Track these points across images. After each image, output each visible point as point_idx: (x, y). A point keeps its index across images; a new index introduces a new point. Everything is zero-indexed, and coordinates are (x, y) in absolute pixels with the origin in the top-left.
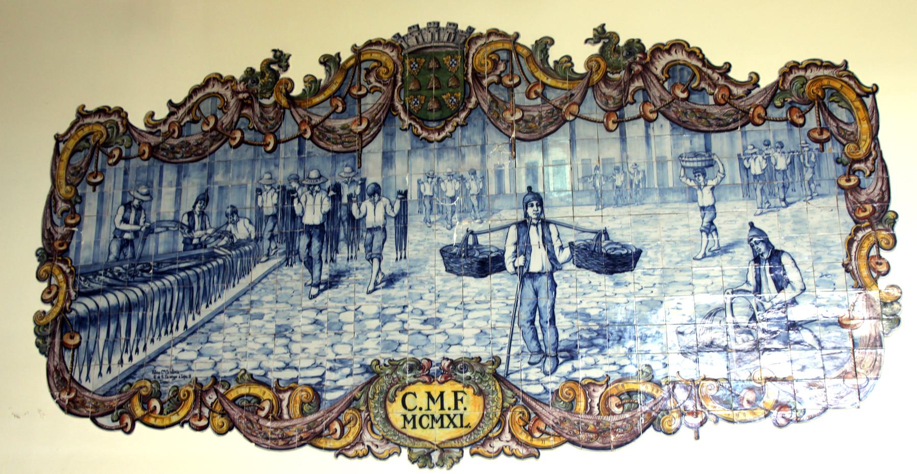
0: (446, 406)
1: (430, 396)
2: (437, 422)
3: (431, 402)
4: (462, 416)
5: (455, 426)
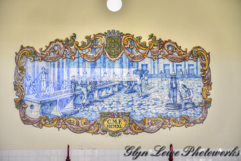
0: (117, 123)
1: (113, 120)
3: (114, 122)
4: (121, 125)
5: (119, 127)
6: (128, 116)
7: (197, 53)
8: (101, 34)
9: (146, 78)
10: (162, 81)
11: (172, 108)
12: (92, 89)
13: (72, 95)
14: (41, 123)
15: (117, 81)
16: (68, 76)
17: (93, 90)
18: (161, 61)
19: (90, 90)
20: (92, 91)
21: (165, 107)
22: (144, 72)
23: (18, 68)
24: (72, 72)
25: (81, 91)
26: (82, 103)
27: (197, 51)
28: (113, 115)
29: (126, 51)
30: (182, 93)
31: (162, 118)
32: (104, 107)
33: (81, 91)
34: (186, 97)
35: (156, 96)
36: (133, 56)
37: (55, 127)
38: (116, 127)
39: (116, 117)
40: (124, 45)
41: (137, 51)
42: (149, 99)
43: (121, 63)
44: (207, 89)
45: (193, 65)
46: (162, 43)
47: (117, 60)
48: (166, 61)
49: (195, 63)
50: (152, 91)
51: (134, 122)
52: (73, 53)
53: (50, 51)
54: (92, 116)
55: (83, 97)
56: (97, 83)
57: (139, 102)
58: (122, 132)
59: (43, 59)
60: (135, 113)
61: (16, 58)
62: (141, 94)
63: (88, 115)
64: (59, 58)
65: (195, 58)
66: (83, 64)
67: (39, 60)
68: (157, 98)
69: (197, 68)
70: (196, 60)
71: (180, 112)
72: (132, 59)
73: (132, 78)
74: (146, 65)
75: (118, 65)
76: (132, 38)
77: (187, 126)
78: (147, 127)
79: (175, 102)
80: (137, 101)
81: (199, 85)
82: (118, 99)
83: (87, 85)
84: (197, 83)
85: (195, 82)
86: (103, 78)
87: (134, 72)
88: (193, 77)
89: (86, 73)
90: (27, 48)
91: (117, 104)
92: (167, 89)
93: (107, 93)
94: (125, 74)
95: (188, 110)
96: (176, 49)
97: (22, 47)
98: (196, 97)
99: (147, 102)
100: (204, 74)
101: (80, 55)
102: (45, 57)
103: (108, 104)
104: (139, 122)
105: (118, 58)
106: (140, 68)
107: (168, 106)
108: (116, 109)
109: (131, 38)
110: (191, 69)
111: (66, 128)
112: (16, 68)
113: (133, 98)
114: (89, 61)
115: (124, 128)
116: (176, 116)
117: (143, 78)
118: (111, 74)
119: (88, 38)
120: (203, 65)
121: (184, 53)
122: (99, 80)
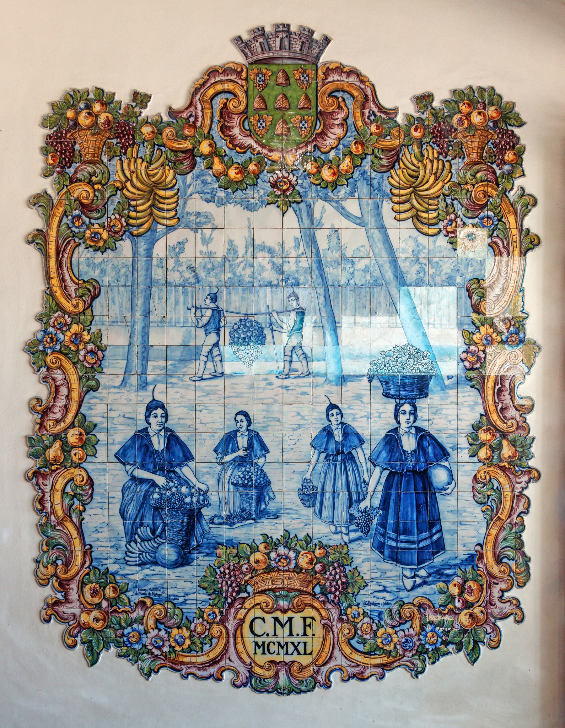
0: (294, 633)
2: (282, 648)
4: (305, 643)
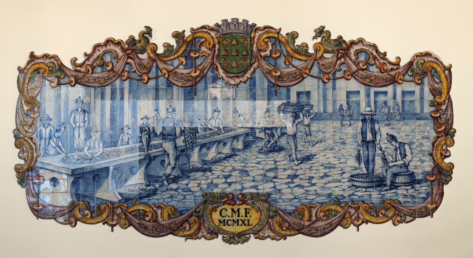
0: (240, 216)
1: (233, 210)
3: (233, 213)
4: (249, 220)
6: (266, 201)
7: (422, 66)
8: (207, 27)
9: (307, 121)
10: (343, 127)
11: (363, 185)
12: (187, 143)
13: (142, 157)
14: (74, 216)
15: (243, 128)
16: (134, 116)
17: (188, 146)
18: (341, 83)
19: (181, 146)
20: (187, 148)
21: (349, 181)
22: (303, 109)
23: (24, 101)
24: (141, 107)
25: (161, 149)
26: (164, 174)
27: (423, 62)
28: (233, 199)
29: (263, 63)
30: (386, 153)
31: (342, 205)
32: (212, 182)
33: (161, 149)
34: (396, 161)
35: (328, 158)
36: (278, 74)
37: (104, 224)
38: (238, 225)
39: (238, 202)
40: (259, 50)
41: (287, 64)
42: (312, 165)
43: (251, 89)
44: (443, 143)
45: (412, 93)
46: (344, 45)
47: (243, 82)
48: (353, 85)
49: (417, 89)
50: (320, 149)
51: (279, 214)
52: (145, 67)
53: (95, 64)
54: (185, 200)
55: (167, 162)
56: (198, 133)
57: (289, 172)
58: (251, 234)
59: (79, 81)
60: (281, 194)
61: (18, 79)
62: (296, 154)
63: (176, 199)
64: (114, 78)
65: (418, 77)
66: (166, 92)
67: (70, 83)
68: (330, 164)
69: (422, 98)
70: (420, 82)
71: (382, 193)
72: (276, 81)
73: (275, 121)
74: (308, 93)
75: (246, 93)
76: (276, 36)
77: (397, 223)
78: (307, 223)
79: (370, 171)
80: (285, 170)
81: (426, 134)
82: (243, 165)
83: (176, 135)
84: (422, 132)
85: (417, 130)
86: (210, 122)
87: (280, 107)
88: (413, 119)
89: (174, 110)
90: (42, 57)
91: (240, 175)
92: (352, 145)
93: (220, 153)
94: (260, 113)
95: (399, 188)
96: (375, 58)
97: (32, 56)
98: (419, 161)
99: (309, 172)
100: (437, 111)
101: (159, 72)
102: (84, 76)
103: (221, 177)
104: (290, 214)
105: (245, 78)
106: (293, 99)
107: (355, 179)
108: (239, 187)
109: (273, 36)
110: (408, 101)
111: (129, 226)
112: (19, 101)
113: (277, 164)
114: (180, 84)
115: (257, 226)
116: (373, 202)
117: (299, 120)
118: (228, 113)
119: (178, 36)
120: (435, 92)
121: (392, 66)
122: (202, 125)
